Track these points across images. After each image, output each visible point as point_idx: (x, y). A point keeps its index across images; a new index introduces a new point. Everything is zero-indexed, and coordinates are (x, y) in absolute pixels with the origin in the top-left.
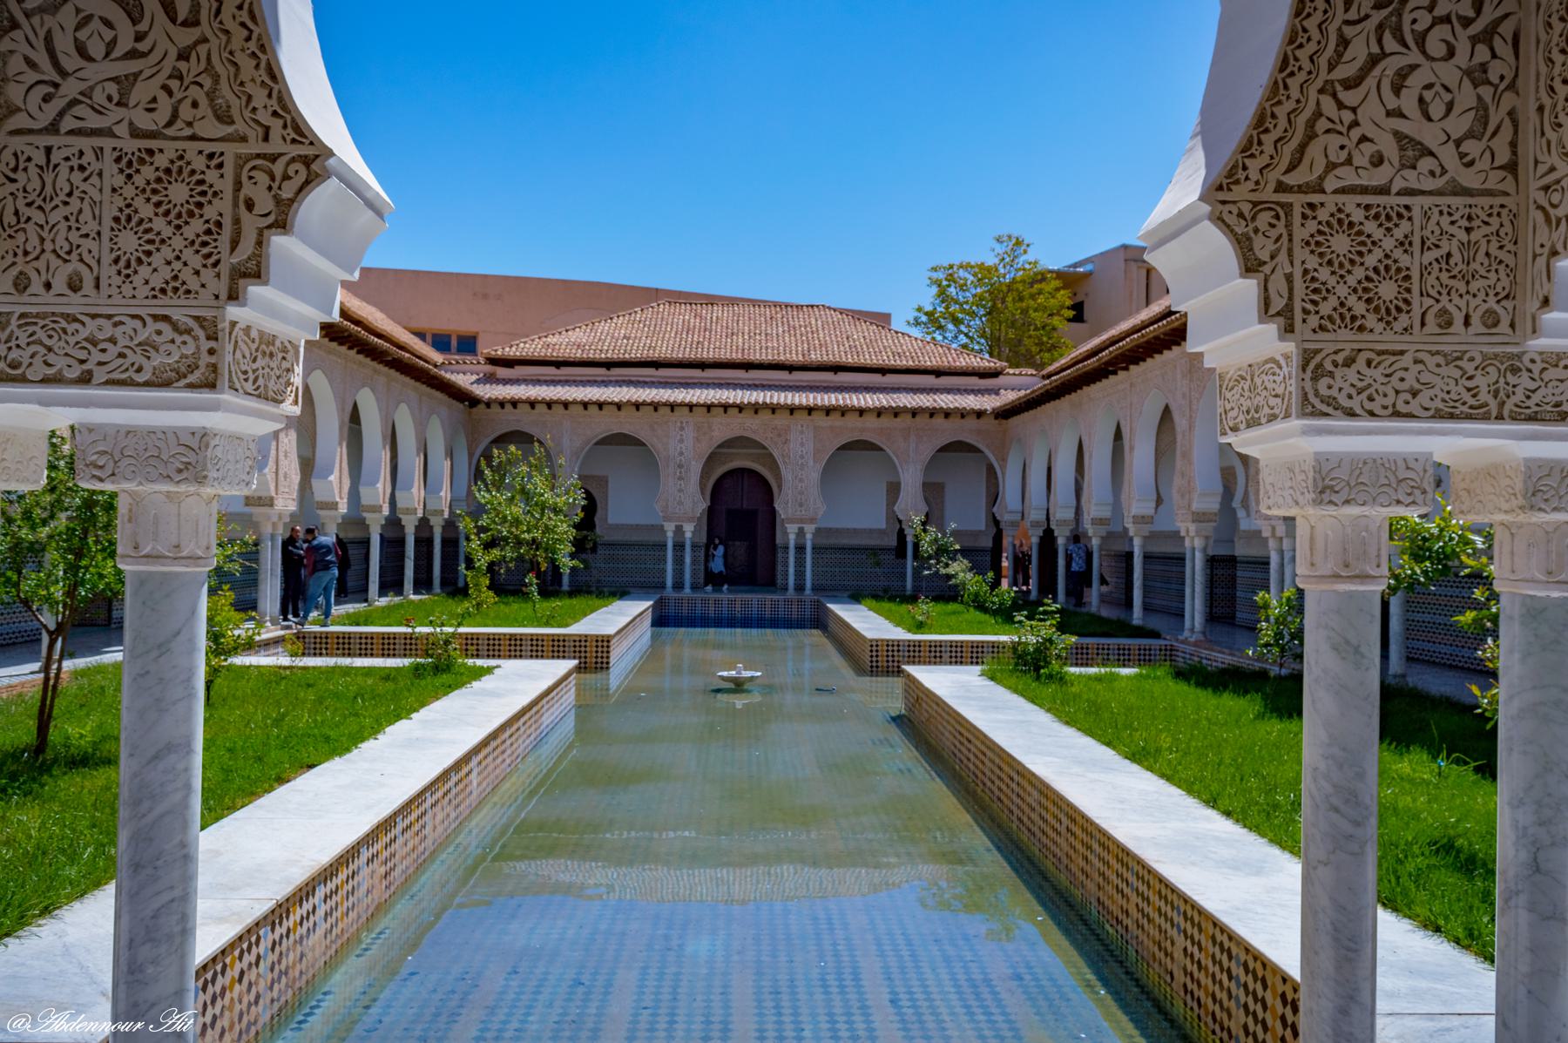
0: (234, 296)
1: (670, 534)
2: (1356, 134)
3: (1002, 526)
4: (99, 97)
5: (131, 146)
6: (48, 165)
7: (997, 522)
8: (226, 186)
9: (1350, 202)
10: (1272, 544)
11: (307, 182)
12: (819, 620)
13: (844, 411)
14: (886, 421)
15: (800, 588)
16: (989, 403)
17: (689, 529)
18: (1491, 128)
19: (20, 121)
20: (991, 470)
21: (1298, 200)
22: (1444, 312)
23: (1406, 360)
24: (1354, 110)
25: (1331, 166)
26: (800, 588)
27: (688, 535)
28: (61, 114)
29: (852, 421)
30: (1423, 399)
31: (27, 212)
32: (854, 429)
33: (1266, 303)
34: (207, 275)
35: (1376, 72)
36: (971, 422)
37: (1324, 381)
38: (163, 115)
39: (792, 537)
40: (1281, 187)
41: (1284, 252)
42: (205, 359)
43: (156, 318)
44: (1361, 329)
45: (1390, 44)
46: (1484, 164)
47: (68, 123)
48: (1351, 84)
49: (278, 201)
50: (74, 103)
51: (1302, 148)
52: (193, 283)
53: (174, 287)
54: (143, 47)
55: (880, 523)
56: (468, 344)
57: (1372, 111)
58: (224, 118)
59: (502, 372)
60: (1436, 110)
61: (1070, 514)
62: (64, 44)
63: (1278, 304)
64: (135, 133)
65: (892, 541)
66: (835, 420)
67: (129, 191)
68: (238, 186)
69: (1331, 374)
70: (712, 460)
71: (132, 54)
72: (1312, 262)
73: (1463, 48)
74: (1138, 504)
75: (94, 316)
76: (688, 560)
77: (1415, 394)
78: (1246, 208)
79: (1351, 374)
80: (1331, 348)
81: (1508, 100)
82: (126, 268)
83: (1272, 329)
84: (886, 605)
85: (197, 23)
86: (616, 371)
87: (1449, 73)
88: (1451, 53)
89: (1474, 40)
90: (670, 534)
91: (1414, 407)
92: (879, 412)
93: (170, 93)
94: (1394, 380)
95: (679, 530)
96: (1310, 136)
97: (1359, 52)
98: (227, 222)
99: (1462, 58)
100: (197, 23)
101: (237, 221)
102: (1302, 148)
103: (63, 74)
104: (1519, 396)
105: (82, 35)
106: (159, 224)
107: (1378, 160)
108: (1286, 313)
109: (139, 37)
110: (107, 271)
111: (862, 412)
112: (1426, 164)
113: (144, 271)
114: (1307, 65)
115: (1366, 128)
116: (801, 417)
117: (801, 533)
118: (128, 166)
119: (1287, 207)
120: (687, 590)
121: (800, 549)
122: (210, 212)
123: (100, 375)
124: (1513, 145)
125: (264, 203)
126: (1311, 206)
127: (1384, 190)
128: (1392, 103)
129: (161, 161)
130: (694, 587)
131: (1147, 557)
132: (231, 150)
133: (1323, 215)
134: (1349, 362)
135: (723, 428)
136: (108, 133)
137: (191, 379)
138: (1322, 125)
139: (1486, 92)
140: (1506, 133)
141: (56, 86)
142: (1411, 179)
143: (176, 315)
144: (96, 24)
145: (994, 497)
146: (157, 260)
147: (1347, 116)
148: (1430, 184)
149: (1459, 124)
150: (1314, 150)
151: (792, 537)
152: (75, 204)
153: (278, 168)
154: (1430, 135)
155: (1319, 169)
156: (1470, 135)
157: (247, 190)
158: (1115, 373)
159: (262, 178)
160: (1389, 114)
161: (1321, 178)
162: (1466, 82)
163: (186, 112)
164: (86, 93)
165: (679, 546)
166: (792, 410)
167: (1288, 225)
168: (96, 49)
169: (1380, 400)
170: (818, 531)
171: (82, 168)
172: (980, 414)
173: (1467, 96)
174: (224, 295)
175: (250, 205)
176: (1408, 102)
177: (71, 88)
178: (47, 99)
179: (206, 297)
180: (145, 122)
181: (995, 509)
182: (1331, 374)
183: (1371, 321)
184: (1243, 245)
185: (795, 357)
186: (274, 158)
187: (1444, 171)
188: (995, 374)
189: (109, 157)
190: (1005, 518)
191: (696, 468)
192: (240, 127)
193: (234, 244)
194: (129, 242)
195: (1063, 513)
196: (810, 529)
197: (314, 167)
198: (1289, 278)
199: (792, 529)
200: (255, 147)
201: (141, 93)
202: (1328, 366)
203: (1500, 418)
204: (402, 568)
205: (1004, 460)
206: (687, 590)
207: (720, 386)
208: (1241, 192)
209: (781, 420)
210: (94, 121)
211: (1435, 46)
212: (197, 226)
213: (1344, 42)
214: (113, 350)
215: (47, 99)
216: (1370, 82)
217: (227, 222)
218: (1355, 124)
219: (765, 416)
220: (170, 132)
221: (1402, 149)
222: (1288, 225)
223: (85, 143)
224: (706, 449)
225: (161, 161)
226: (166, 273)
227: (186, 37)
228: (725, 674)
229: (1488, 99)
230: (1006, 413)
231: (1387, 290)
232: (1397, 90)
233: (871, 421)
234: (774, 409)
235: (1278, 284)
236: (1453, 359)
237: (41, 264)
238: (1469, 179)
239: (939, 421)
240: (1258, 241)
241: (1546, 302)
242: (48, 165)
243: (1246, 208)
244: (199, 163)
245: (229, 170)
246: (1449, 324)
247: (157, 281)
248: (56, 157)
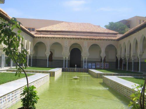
1: (64, 58)
3: (118, 58)
7: (117, 58)
12: (87, 71)
14: (99, 41)
17: (67, 58)
20: (116, 49)
27: (67, 59)
32: (94, 42)
36: (113, 41)
56: (33, 30)
61: (129, 55)
65: (100, 60)
70: (71, 47)
74: (139, 52)
90: (64, 58)
92: (98, 39)
95: (66, 58)
111: (95, 39)
117: (85, 59)
120: (67, 67)
130: (68, 67)
135: (73, 42)
151: (84, 59)
158: (136, 32)
165: (66, 61)
185: (84, 31)
190: (118, 57)
191: (69, 48)
195: (127, 55)
196: (87, 58)
199: (84, 58)
206: (67, 67)
209: (82, 41)
224: (70, 45)
228: (73, 77)
233: (97, 41)
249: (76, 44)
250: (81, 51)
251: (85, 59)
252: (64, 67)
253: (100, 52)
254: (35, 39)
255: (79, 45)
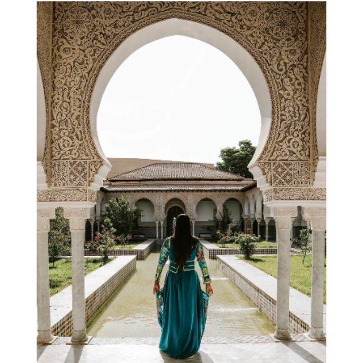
0: (89, 186)
2: (282, 150)
3: (244, 220)
4: (67, 153)
5: (72, 161)
6: (59, 165)
8: (88, 167)
9: (281, 162)
10: (308, 223)
11: (101, 166)
13: (201, 191)
14: (213, 193)
16: (240, 188)
17: (162, 223)
18: (305, 149)
19: (54, 158)
21: (272, 162)
22: (298, 182)
23: (291, 190)
24: (281, 146)
25: (278, 156)
27: (162, 224)
28: (61, 156)
29: (204, 193)
30: (295, 196)
31: (56, 173)
32: (204, 195)
33: (267, 180)
34: (85, 182)
35: (285, 140)
36: (235, 193)
37: (277, 194)
38: (77, 155)
40: (269, 160)
41: (270, 172)
42: (85, 196)
43: (77, 190)
44: (284, 185)
45: (287, 134)
46: (304, 155)
47: (62, 158)
48: (280, 142)
49: (96, 169)
50: (63, 154)
51: (273, 153)
52: (83, 184)
53: (80, 184)
54: (74, 144)
55: (212, 219)
57: (285, 146)
58: (87, 155)
59: (113, 184)
60: (296, 146)
62: (61, 145)
63: (269, 180)
64: (73, 159)
66: (199, 193)
67: (72, 169)
68: (89, 167)
69: (279, 193)
71: (72, 146)
72: (275, 173)
73: (300, 135)
75: (67, 190)
76: (162, 230)
77: (293, 196)
78: (263, 164)
79: (282, 192)
80: (278, 188)
81: (308, 144)
82: (72, 181)
83: (268, 184)
85: (82, 140)
86: (142, 182)
87: (298, 139)
88: (298, 136)
89: (302, 134)
91: (293, 198)
92: (211, 191)
93: (78, 152)
94: (289, 194)
96: (274, 151)
97: (282, 136)
98: (88, 173)
99: (300, 137)
100: (82, 140)
101: (89, 173)
102: (273, 153)
103: (61, 150)
104: (311, 196)
105: (64, 143)
106: (77, 174)
107: (286, 155)
108: (271, 182)
109: (73, 143)
110: (69, 183)
111: (206, 191)
112: (294, 155)
113: (75, 182)
114: (273, 138)
115: (284, 149)
116: (190, 193)
118: (72, 164)
119: (270, 163)
122: (85, 171)
123: (68, 199)
124: (309, 152)
125: (94, 169)
126: (275, 163)
127: (287, 160)
128: (288, 145)
129: (77, 163)
131: (269, 226)
132: (88, 161)
133: (276, 165)
134: (281, 190)
135: (170, 196)
136: (68, 159)
137: (83, 199)
138: (276, 149)
139: (304, 143)
140: (308, 150)
141: (60, 152)
142: (292, 158)
143: (81, 189)
144: (66, 141)
145: (241, 211)
146: (77, 180)
147: (280, 148)
148: (296, 159)
149: (300, 148)
150: (275, 153)
152: (63, 171)
153: (96, 164)
154: (295, 150)
155: (275, 157)
156: (302, 150)
157: (91, 167)
159: (93, 165)
160: (288, 147)
161: (276, 158)
162: (301, 141)
163: (81, 155)
164: (65, 153)
165: (160, 227)
166: (188, 191)
167: (270, 166)
168: (66, 145)
169: (287, 197)
171: (64, 165)
172: (237, 191)
173: (301, 143)
174: (88, 185)
175: (91, 170)
176: (291, 145)
177: (62, 152)
178: (59, 154)
179: (85, 186)
180: (74, 157)
181: (242, 215)
182: (279, 193)
183: (285, 183)
184: (263, 170)
185: (188, 176)
186: (95, 162)
187: (297, 157)
188: (241, 180)
189: (69, 163)
191: (163, 206)
192: (90, 157)
193: (89, 177)
194: (72, 177)
197: (102, 163)
198: (271, 176)
200: (92, 160)
201: (74, 152)
202: (278, 191)
203: (308, 200)
204: (91, 234)
205: (244, 203)
207: (169, 185)
208: (262, 161)
209: (185, 194)
210: (66, 157)
211: (295, 135)
212: (83, 174)
213: (279, 134)
214: (70, 195)
215: (59, 154)
216: (284, 141)
217: (88, 173)
218: (282, 149)
219: (181, 193)
220: (79, 158)
221: (290, 153)
222: (270, 166)
223: (65, 161)
224: (166, 201)
225: (77, 163)
226: (78, 182)
227: (80, 142)
229: (305, 144)
230: (244, 191)
231: (288, 178)
232: (289, 142)
233: (209, 193)
234: (183, 191)
235: (269, 177)
236: (300, 190)
237: (58, 181)
238: (302, 158)
239: (227, 193)
240: (266, 169)
241: (314, 180)
242: (59, 165)
243: (263, 164)
244: (83, 163)
245: (88, 164)
246: (299, 183)
247: (77, 183)
248: (60, 164)
249: (175, 200)
253: (215, 211)
254: (108, 194)
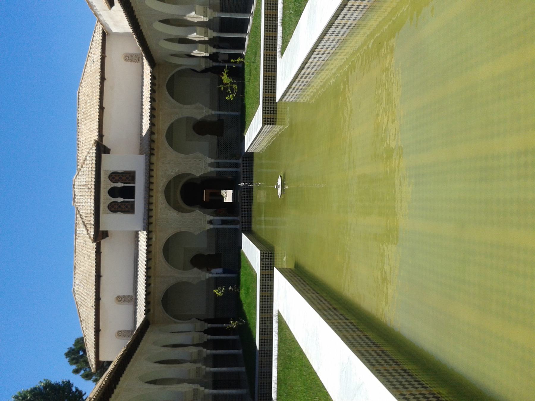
15: (237, 165)
17: (209, 218)
26: (237, 165)
32: (161, 138)
39: (213, 169)
84: (247, 120)
95: (210, 222)
117: (211, 165)
121: (218, 165)
151: (213, 169)
170: (211, 156)
190: (203, 66)
196: (210, 160)
199: (210, 169)
250: (190, 177)
251: (211, 165)
252: (238, 226)
255: (170, 181)
